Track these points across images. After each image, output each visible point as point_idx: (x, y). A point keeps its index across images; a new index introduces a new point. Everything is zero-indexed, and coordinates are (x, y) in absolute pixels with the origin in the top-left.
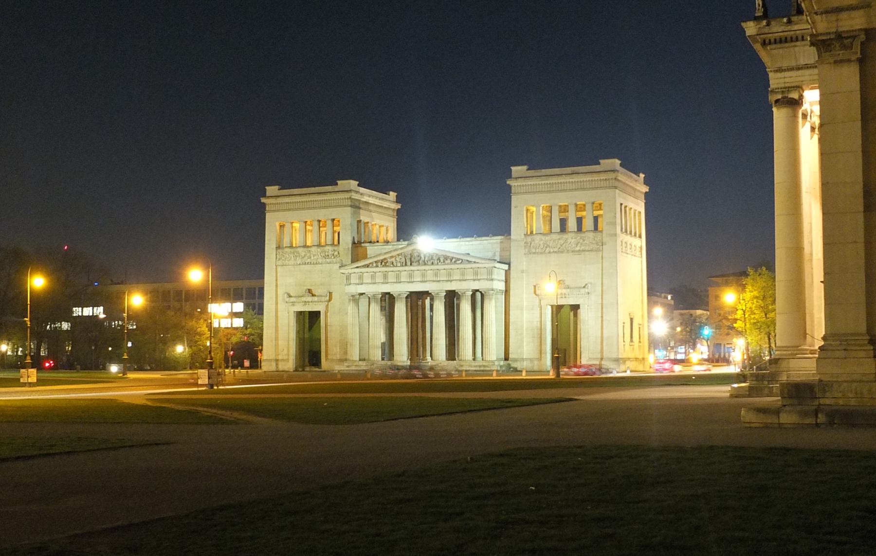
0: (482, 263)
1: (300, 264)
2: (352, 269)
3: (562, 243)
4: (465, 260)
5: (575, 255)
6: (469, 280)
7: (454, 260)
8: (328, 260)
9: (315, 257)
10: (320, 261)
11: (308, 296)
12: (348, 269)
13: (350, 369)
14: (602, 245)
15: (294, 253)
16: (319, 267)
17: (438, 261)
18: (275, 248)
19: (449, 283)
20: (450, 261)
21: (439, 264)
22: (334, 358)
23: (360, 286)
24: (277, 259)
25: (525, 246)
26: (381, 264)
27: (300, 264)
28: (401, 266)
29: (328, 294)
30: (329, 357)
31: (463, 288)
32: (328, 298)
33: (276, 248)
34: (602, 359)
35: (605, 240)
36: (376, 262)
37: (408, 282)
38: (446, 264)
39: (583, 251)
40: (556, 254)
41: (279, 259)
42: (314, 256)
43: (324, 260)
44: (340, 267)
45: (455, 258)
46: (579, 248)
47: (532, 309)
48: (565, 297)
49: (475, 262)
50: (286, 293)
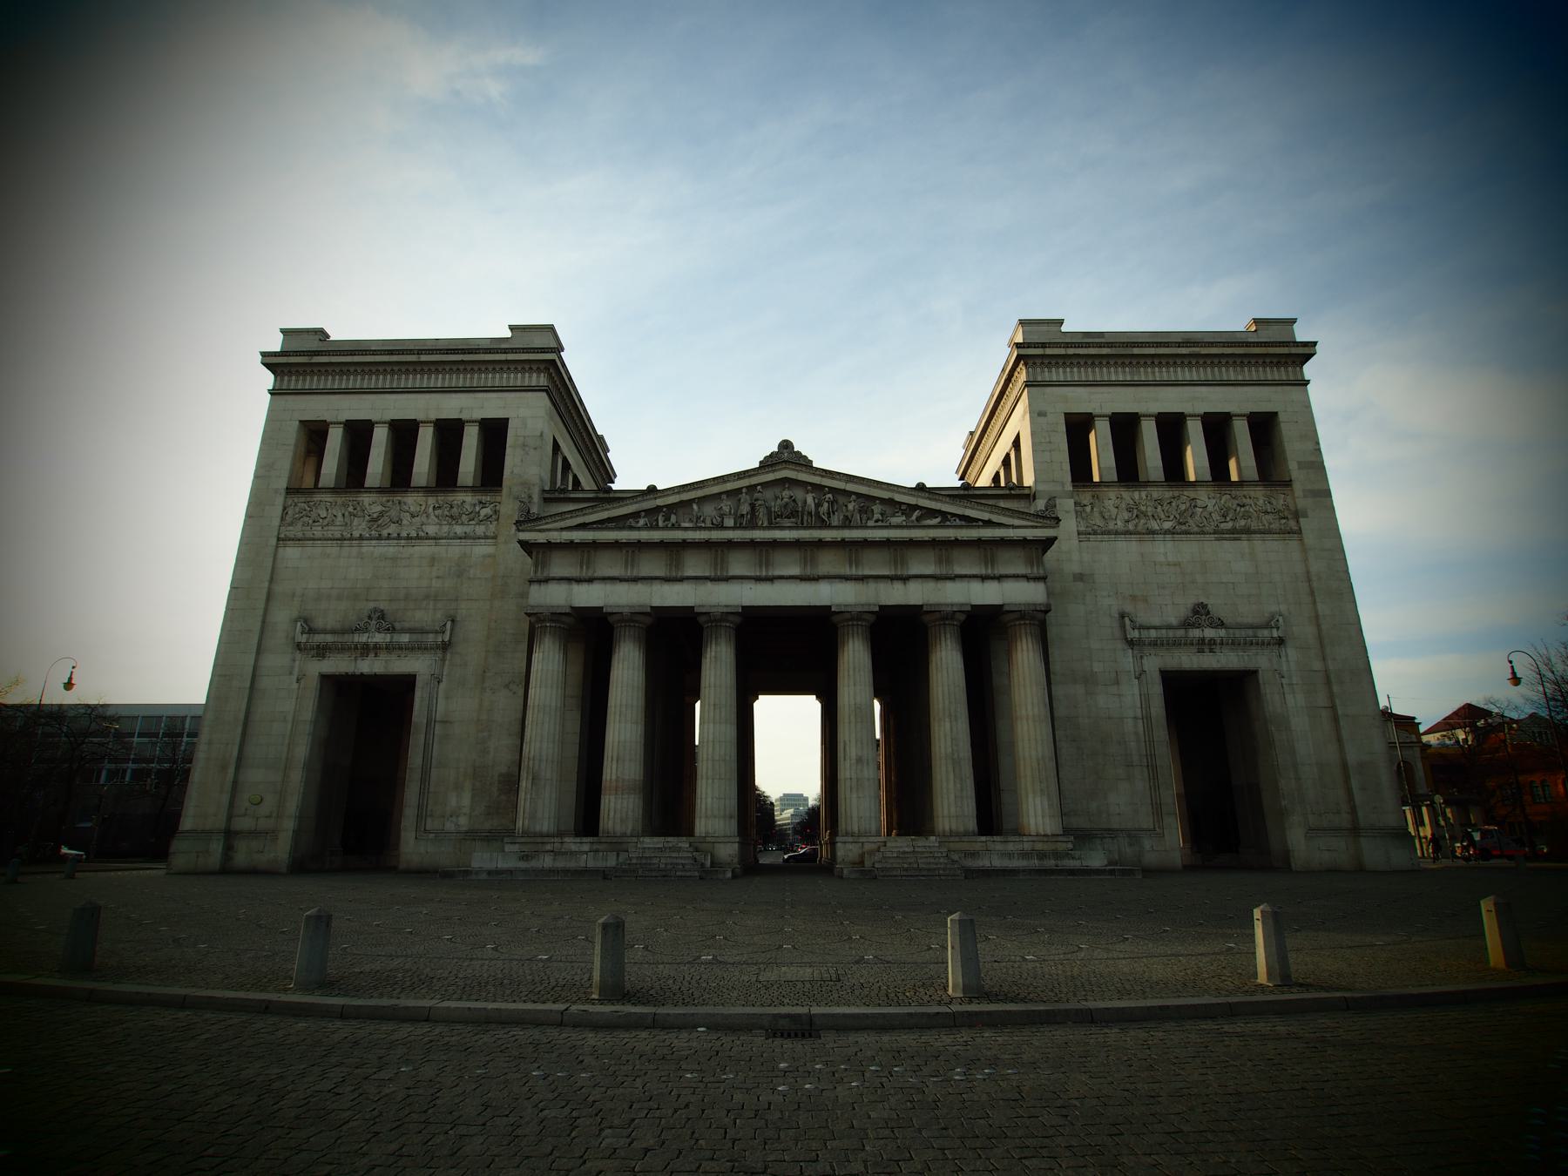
0: (1014, 527)
1: (361, 538)
2: (562, 529)
3: (1183, 507)
4: (954, 515)
5: (1226, 539)
6: (965, 576)
8: (459, 530)
10: (431, 530)
13: (534, 864)
15: (345, 505)
16: (425, 549)
17: (865, 516)
18: (283, 492)
19: (898, 585)
20: (904, 518)
21: (871, 523)
22: (450, 826)
24: (288, 519)
25: (1076, 512)
26: (667, 519)
27: (361, 538)
28: (734, 528)
29: (449, 624)
30: (431, 824)
31: (949, 601)
33: (287, 488)
34: (1355, 830)
35: (1302, 503)
36: (649, 512)
37: (758, 579)
38: (891, 527)
39: (1248, 531)
40: (1168, 537)
41: (291, 524)
42: (413, 516)
43: (445, 529)
44: (518, 523)
45: (921, 508)
46: (1230, 525)
47: (1117, 682)
48: (1211, 651)
49: (988, 524)
50: (296, 621)
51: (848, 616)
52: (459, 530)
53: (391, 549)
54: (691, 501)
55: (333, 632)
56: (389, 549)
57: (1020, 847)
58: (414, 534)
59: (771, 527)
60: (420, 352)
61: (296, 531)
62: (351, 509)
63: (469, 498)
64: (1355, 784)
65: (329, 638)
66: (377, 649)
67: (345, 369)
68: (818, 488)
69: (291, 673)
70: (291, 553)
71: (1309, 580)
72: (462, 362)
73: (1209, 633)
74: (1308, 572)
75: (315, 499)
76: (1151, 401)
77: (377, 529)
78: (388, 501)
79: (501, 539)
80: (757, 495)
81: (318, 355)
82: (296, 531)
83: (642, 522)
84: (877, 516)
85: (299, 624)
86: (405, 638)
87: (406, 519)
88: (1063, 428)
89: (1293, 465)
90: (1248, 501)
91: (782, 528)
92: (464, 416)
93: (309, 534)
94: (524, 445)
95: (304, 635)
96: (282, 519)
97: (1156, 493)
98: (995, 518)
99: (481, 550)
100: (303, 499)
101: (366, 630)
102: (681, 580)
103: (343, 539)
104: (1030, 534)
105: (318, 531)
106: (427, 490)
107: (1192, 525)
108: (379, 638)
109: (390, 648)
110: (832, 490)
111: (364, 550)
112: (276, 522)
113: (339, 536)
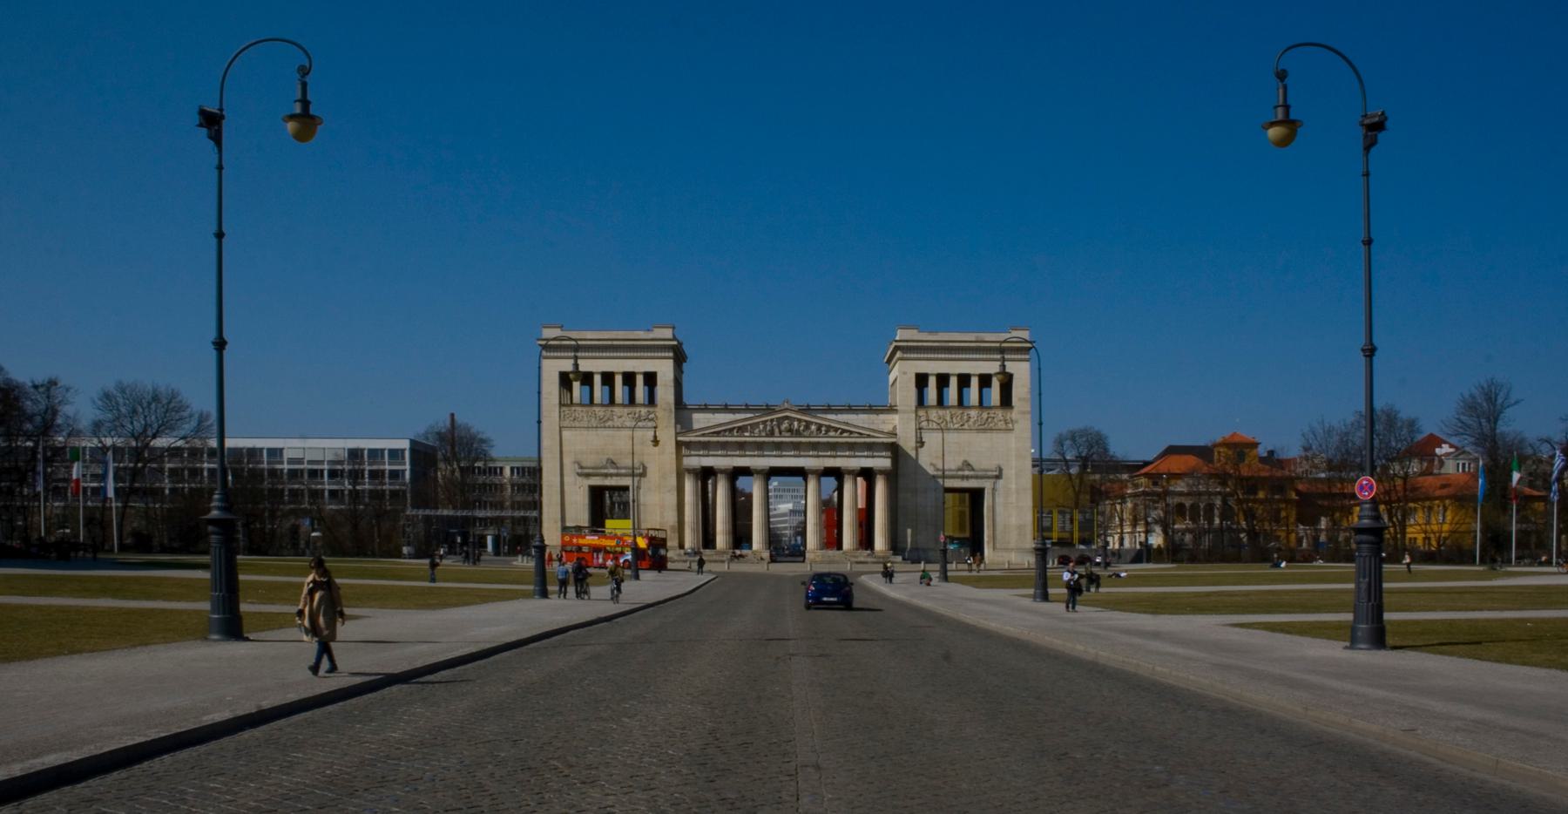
2: (697, 436)
7: (839, 431)
19: (832, 459)
21: (821, 435)
23: (706, 458)
27: (596, 427)
32: (641, 471)
39: (991, 429)
49: (869, 436)
50: (575, 462)
53: (611, 432)
54: (747, 425)
56: (610, 432)
63: (644, 411)
65: (591, 471)
66: (612, 475)
68: (800, 421)
73: (967, 473)
76: (954, 367)
77: (603, 424)
80: (774, 423)
82: (566, 423)
83: (727, 433)
84: (823, 432)
86: (623, 471)
87: (615, 417)
88: (913, 380)
90: (992, 415)
92: (636, 370)
93: (573, 425)
94: (665, 385)
97: (953, 411)
98: (872, 434)
103: (588, 427)
104: (885, 440)
105: (577, 424)
106: (623, 405)
107: (966, 427)
108: (612, 471)
109: (617, 475)
110: (806, 421)
111: (599, 432)
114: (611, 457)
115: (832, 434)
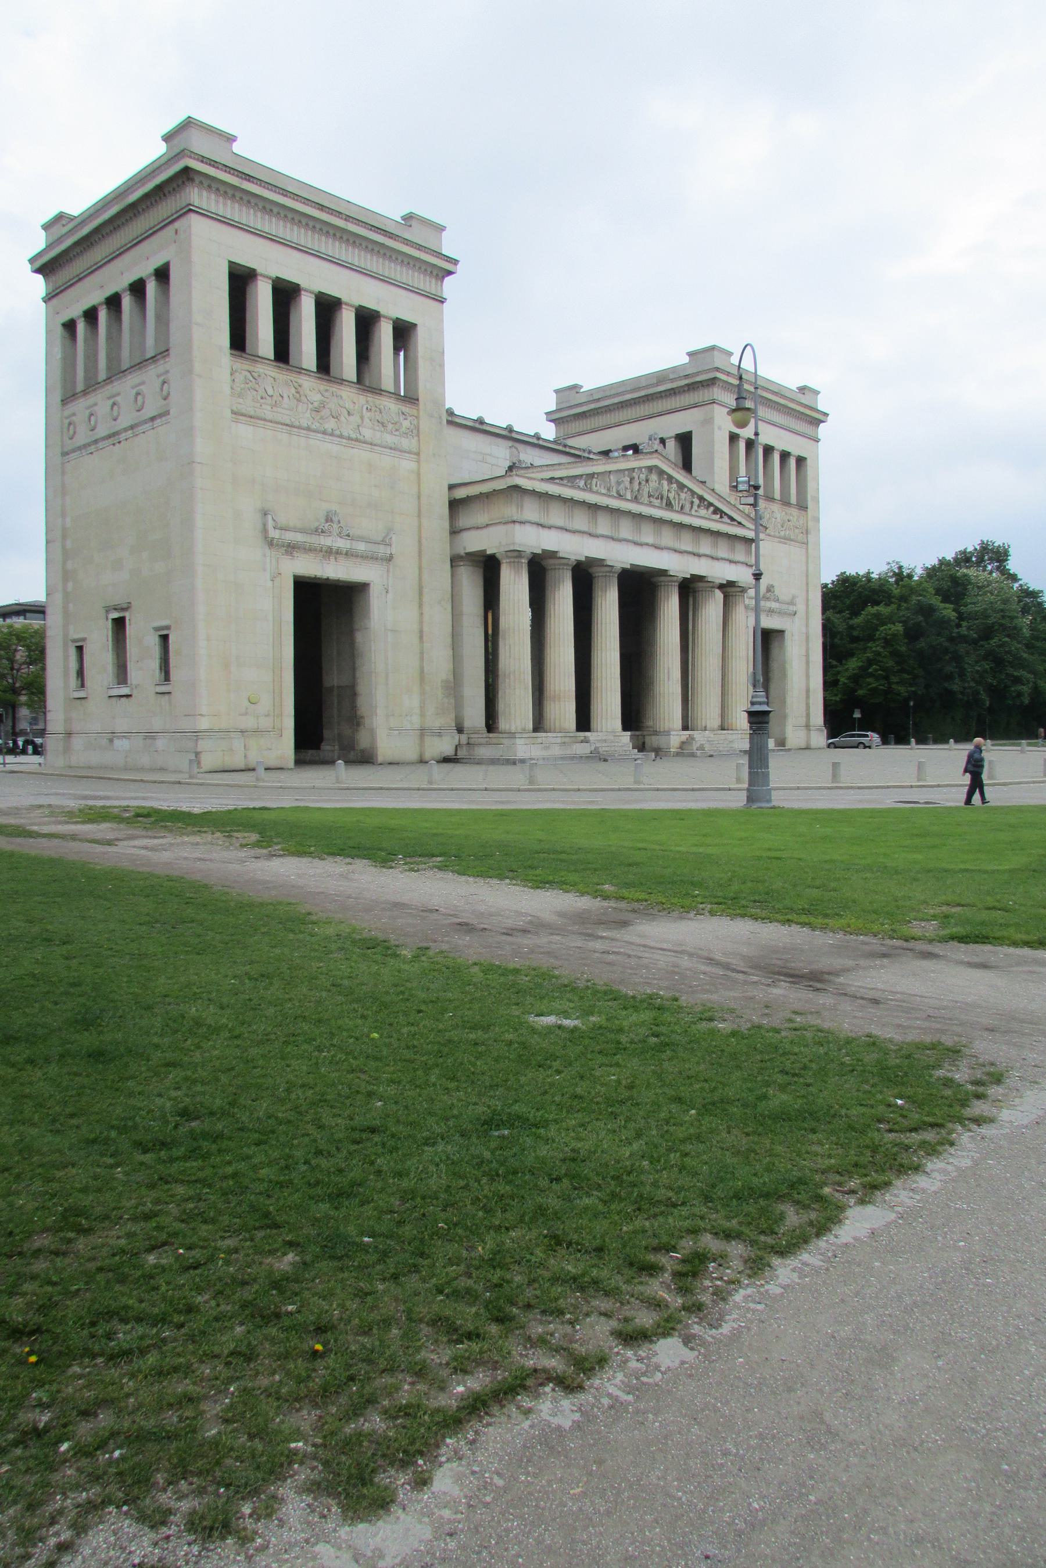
1: (308, 429)
4: (726, 514)
8: (390, 439)
9: (351, 419)
10: (367, 433)
11: (340, 535)
12: (534, 479)
14: (807, 533)
16: (361, 454)
19: (696, 558)
21: (693, 512)
27: (308, 429)
34: (807, 726)
37: (636, 543)
42: (349, 413)
43: (378, 434)
46: (782, 534)
49: (740, 523)
51: (675, 579)
52: (390, 439)
55: (296, 530)
57: (723, 737)
58: (353, 436)
59: (650, 505)
60: (348, 218)
61: (247, 405)
62: (293, 391)
63: (391, 406)
64: (811, 701)
65: (299, 538)
67: (268, 207)
68: (670, 479)
69: (264, 570)
70: (245, 431)
71: (807, 576)
72: (382, 245)
74: (807, 571)
75: (256, 370)
78: (327, 391)
79: (423, 456)
81: (249, 181)
83: (582, 483)
85: (270, 517)
86: (361, 547)
89: (809, 498)
91: (654, 506)
92: (382, 310)
95: (277, 531)
96: (232, 388)
98: (744, 522)
99: (407, 465)
100: (246, 367)
101: (330, 534)
102: (597, 536)
108: (342, 544)
109: (349, 554)
110: (677, 482)
111: (312, 442)
112: (227, 390)
113: (288, 422)
114: (334, 507)
115: (703, 512)
